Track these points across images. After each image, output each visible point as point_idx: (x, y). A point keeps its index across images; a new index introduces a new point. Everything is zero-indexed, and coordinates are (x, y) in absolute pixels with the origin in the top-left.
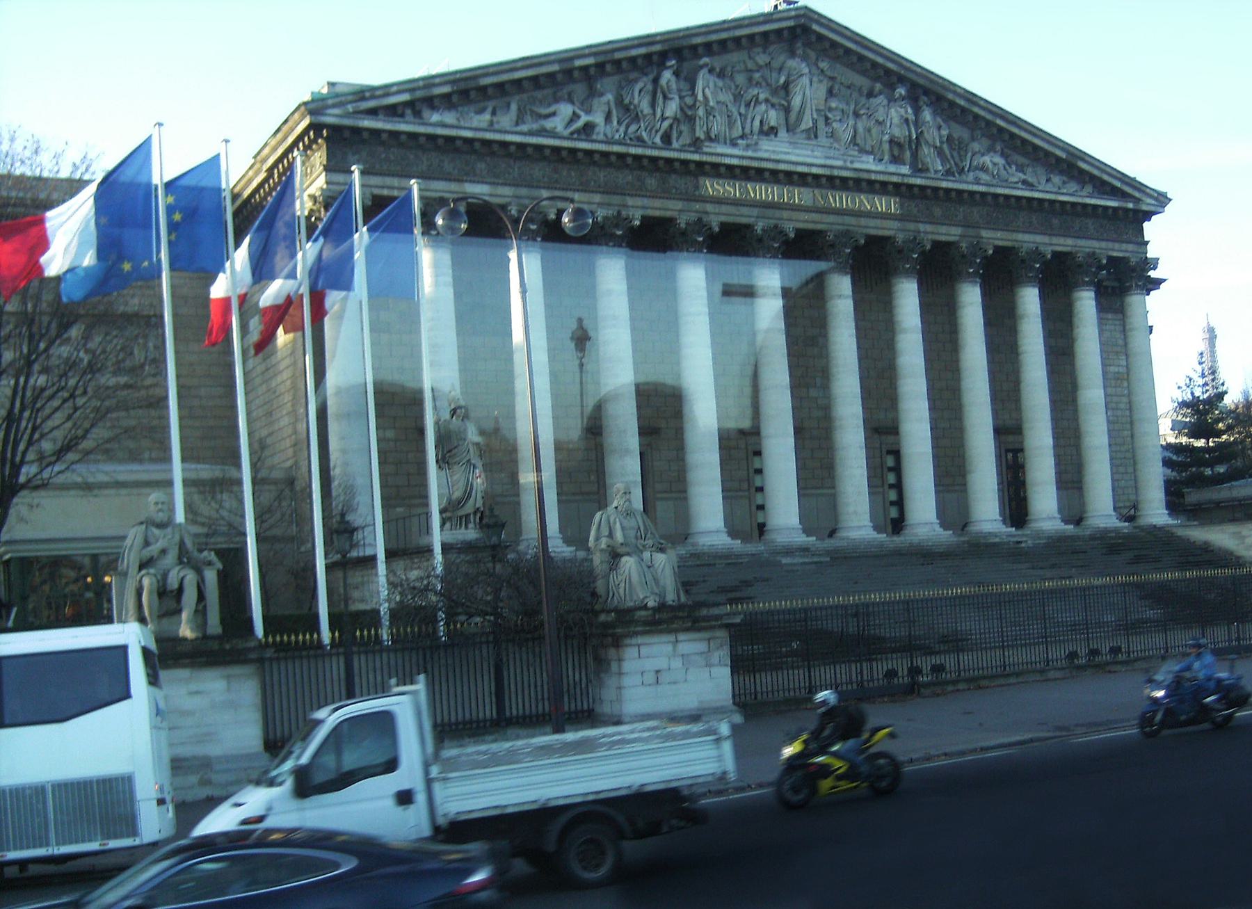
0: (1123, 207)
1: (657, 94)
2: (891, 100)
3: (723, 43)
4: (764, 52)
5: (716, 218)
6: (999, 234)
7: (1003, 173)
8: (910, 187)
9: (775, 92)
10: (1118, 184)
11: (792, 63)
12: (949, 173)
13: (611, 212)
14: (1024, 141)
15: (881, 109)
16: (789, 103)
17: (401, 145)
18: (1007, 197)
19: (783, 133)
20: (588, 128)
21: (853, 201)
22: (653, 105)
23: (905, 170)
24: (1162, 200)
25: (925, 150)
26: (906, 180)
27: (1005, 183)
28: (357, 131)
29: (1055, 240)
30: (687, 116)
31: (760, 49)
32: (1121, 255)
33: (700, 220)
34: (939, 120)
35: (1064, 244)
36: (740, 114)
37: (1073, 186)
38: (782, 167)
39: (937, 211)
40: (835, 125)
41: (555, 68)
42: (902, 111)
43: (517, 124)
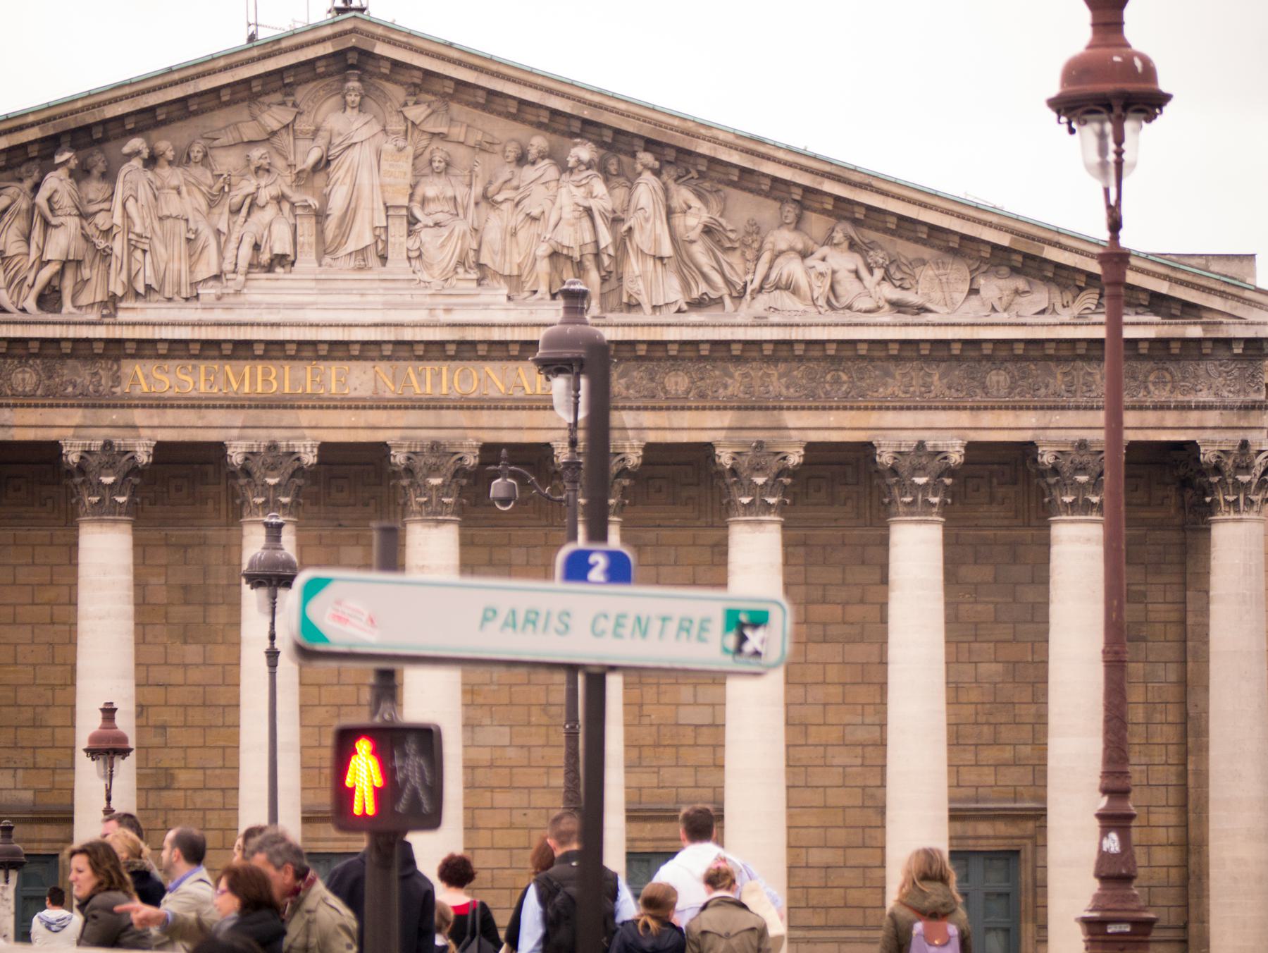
2: (564, 168)
4: (283, 103)
6: (832, 418)
7: (848, 287)
10: (1163, 288)
12: (698, 304)
15: (539, 193)
16: (325, 199)
21: (465, 379)
25: (634, 266)
29: (987, 419)
31: (278, 97)
33: (108, 445)
34: (683, 195)
37: (1041, 296)
39: (677, 382)
40: (426, 236)
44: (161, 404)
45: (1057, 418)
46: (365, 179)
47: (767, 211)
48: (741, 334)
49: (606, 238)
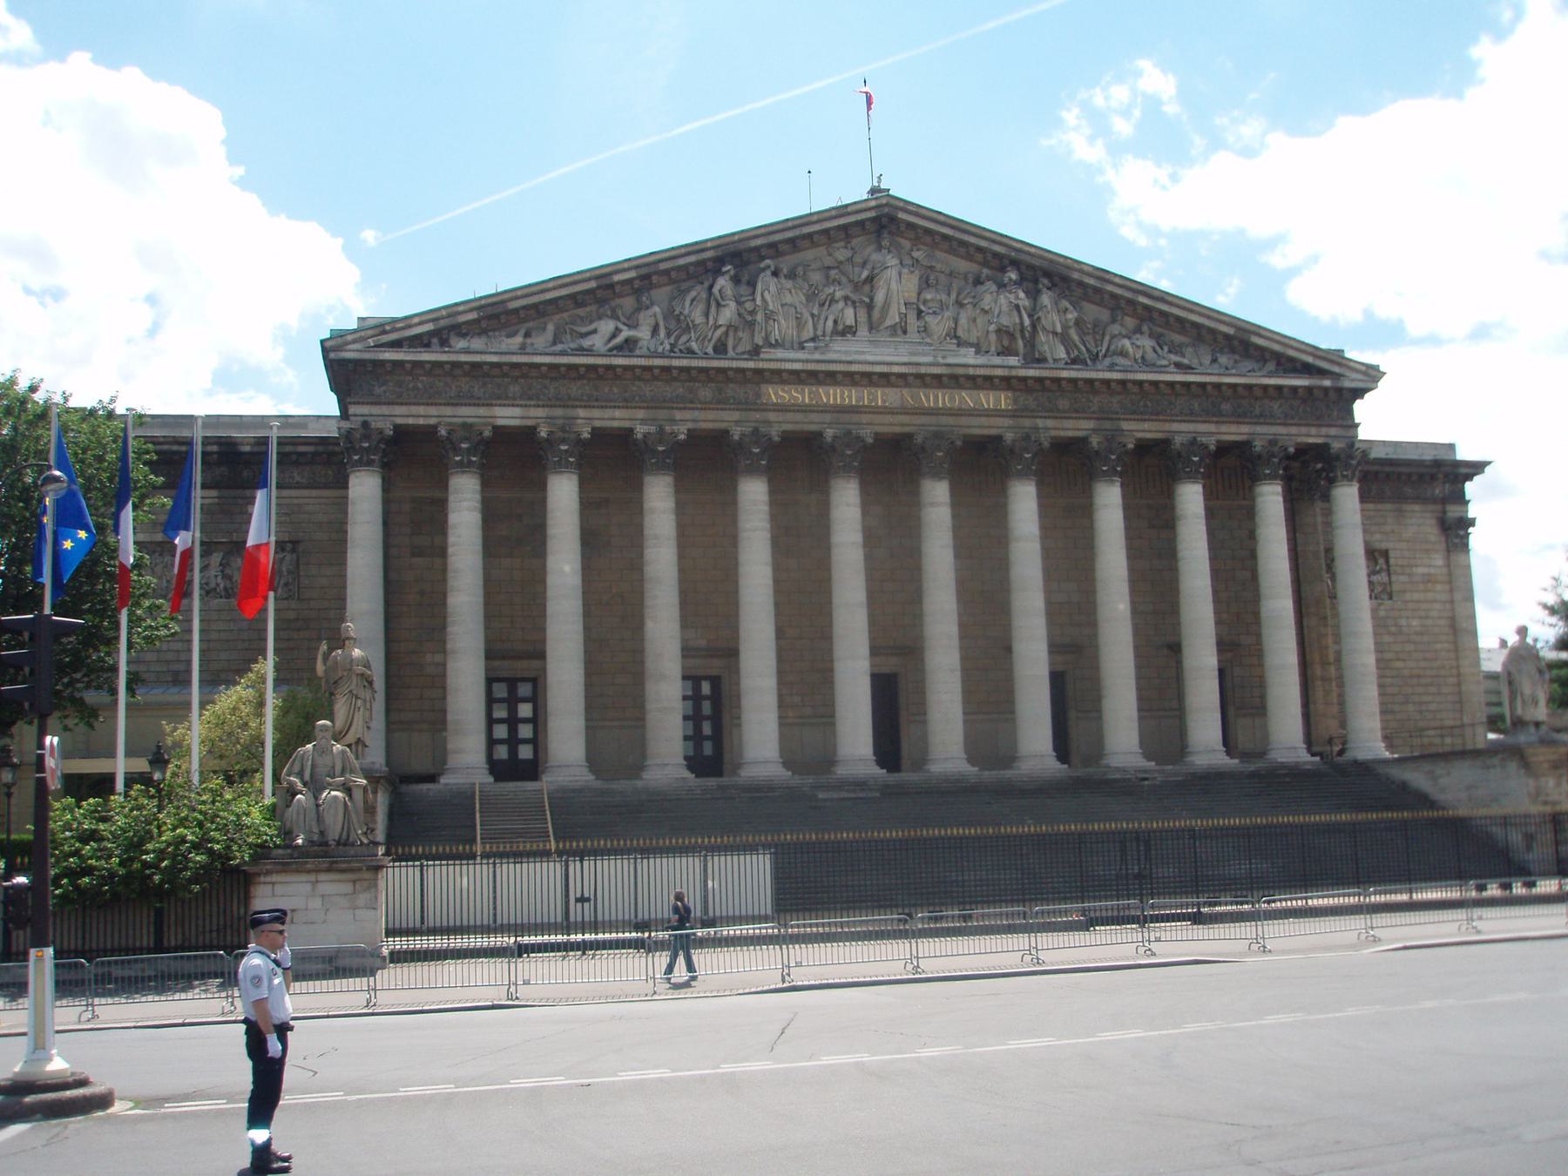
0: (1330, 384)
1: (713, 302)
2: (1001, 286)
3: (792, 241)
5: (778, 426)
6: (1146, 426)
7: (1151, 355)
8: (1024, 379)
9: (857, 287)
10: (1310, 359)
11: (875, 257)
12: (1074, 361)
13: (653, 429)
14: (1179, 320)
15: (988, 298)
16: (872, 299)
17: (429, 373)
18: (1155, 384)
19: (863, 332)
20: (629, 345)
21: (952, 399)
22: (707, 315)
23: (1013, 361)
24: (1372, 376)
25: (1042, 337)
26: (1014, 373)
28: (382, 363)
29: (1224, 428)
32: (1320, 441)
33: (756, 429)
34: (1065, 303)
35: (1233, 432)
36: (813, 315)
37: (1248, 365)
38: (854, 368)
39: (1063, 403)
41: (593, 284)
42: (1012, 297)
43: (554, 343)
44: (782, 408)
45: (1259, 429)
46: (894, 285)
47: (1105, 315)
48: (1101, 375)
49: (1027, 322)
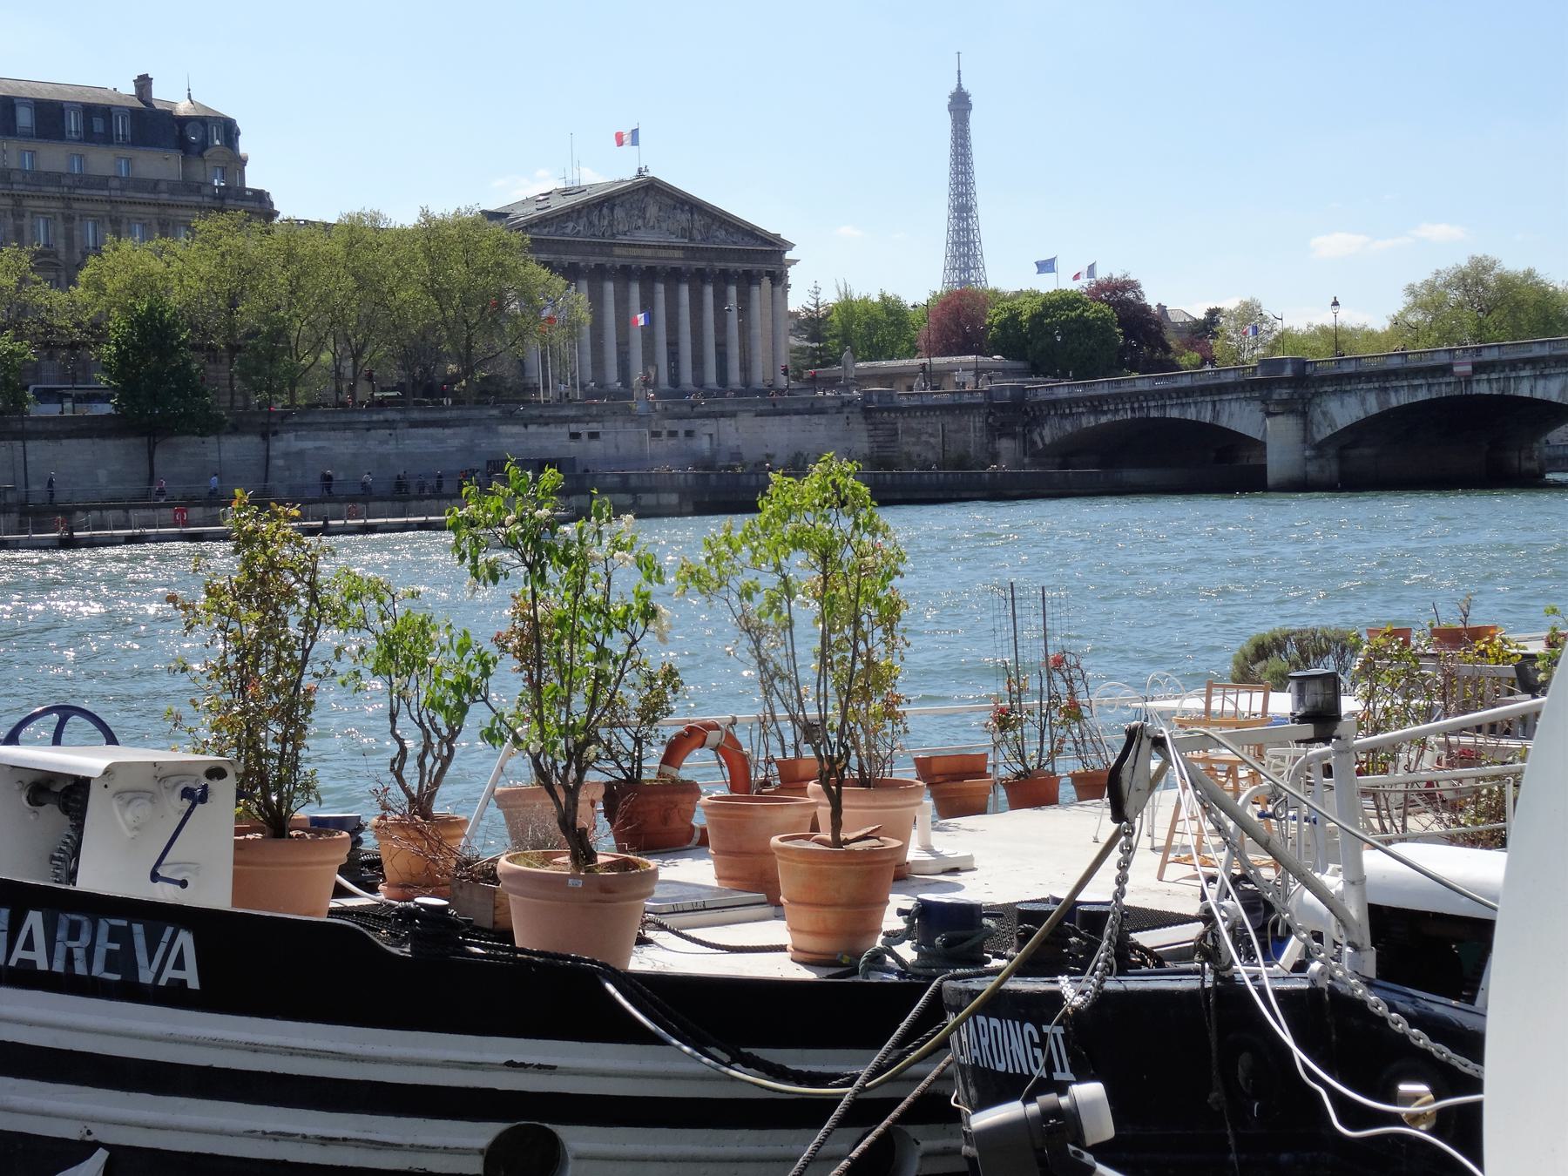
1: (601, 217)
5: (619, 263)
24: (791, 246)
27: (725, 243)
30: (611, 225)
35: (748, 266)
